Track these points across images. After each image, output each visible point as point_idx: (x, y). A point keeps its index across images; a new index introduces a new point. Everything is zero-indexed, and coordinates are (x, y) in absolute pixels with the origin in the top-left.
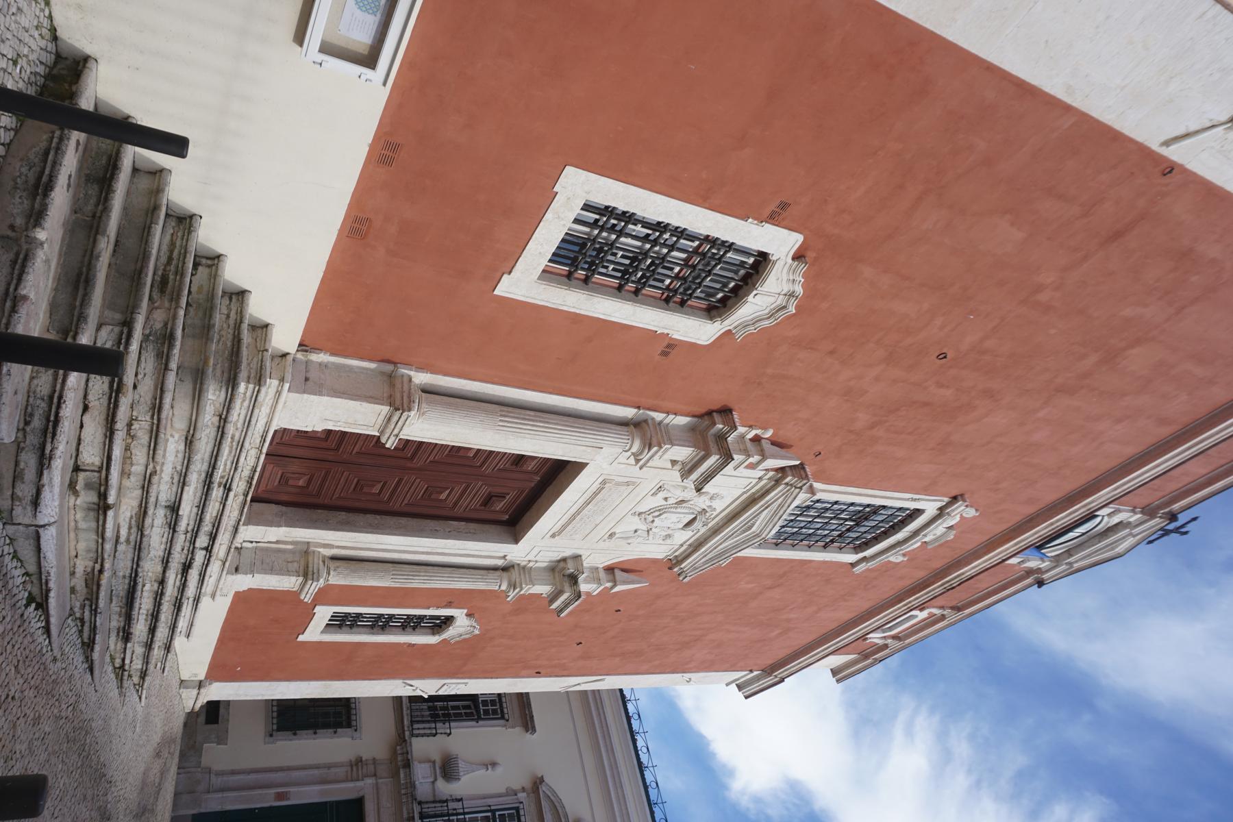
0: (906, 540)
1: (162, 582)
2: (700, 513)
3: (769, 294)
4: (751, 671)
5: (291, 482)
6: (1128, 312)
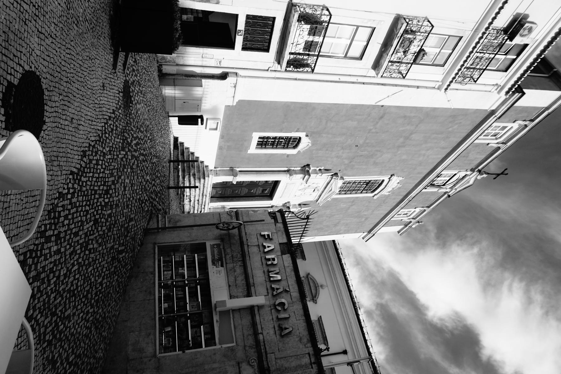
6: (401, 129)
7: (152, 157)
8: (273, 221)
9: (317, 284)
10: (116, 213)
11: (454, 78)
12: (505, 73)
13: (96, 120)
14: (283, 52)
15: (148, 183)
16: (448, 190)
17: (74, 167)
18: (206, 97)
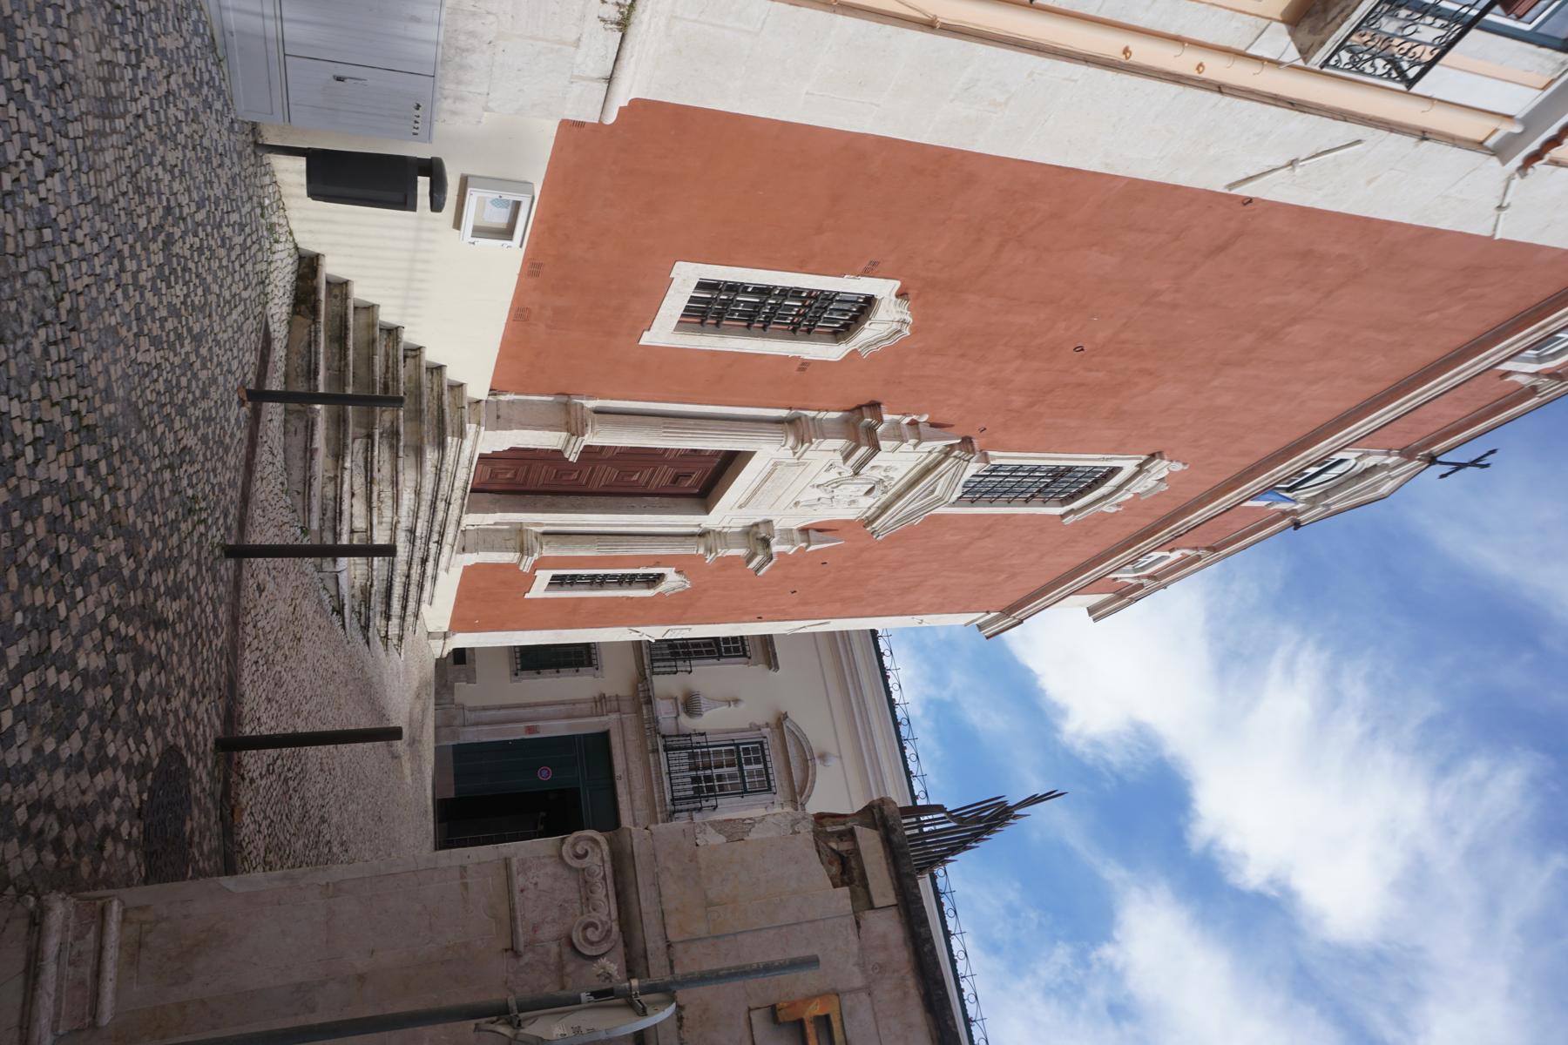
0: (1111, 494)
1: (408, 576)
2: (878, 482)
3: (883, 322)
4: (988, 612)
5: (500, 476)
9: (811, 749)
16: (1299, 506)
18: (462, 67)
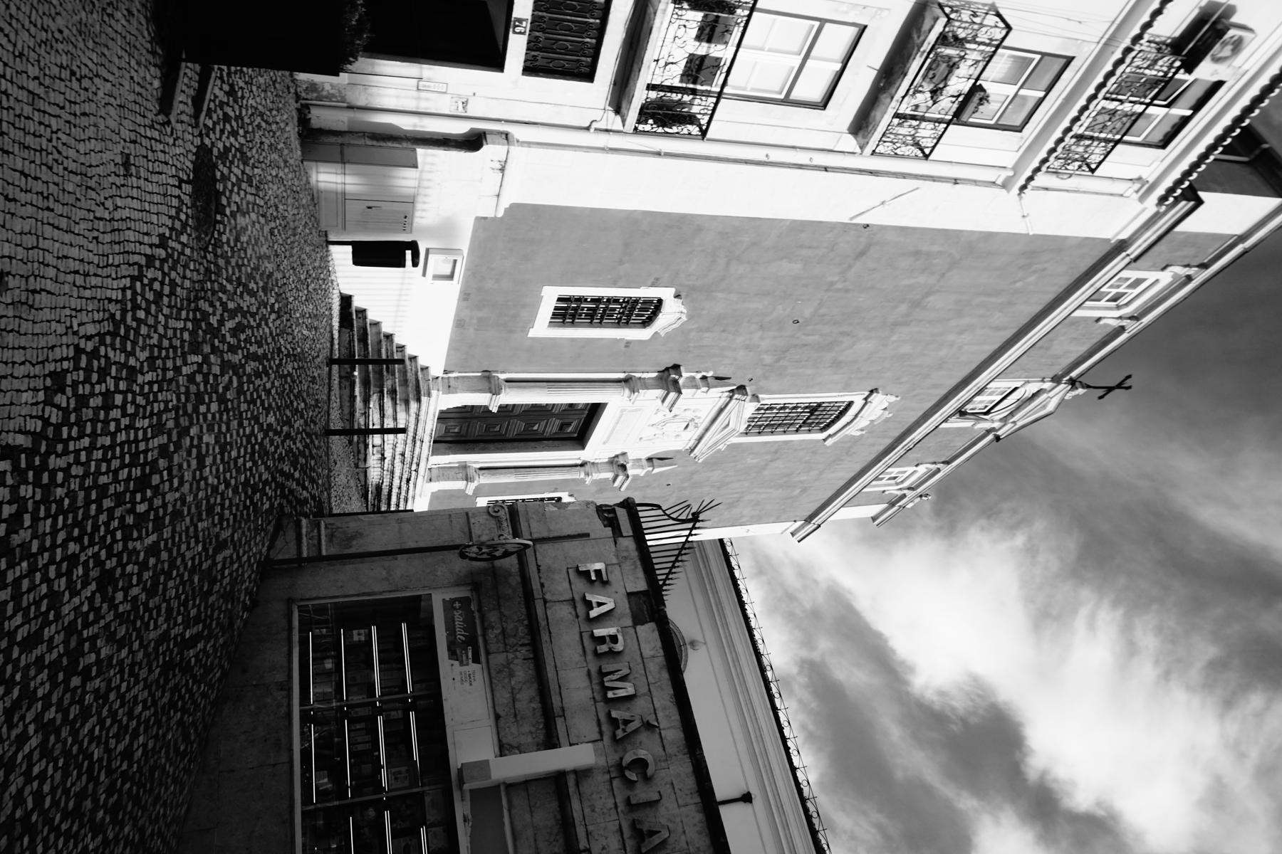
6: (906, 282)
7: (281, 360)
8: (609, 531)
9: (683, 638)
10: (173, 537)
11: (1045, 161)
12: (1160, 151)
13: (99, 271)
14: (631, 83)
15: (271, 434)
16: (996, 425)
17: (20, 432)
18: (425, 195)
